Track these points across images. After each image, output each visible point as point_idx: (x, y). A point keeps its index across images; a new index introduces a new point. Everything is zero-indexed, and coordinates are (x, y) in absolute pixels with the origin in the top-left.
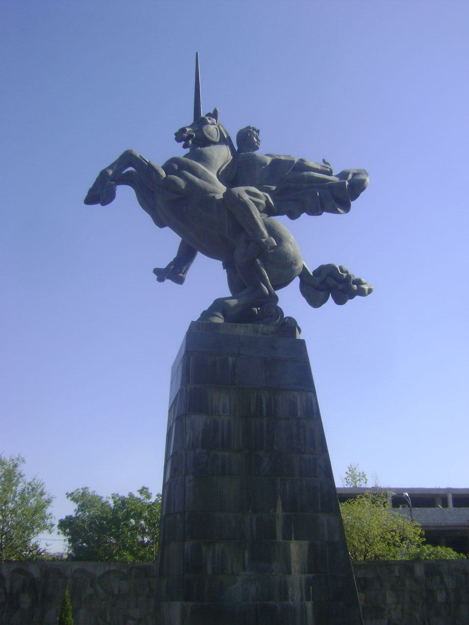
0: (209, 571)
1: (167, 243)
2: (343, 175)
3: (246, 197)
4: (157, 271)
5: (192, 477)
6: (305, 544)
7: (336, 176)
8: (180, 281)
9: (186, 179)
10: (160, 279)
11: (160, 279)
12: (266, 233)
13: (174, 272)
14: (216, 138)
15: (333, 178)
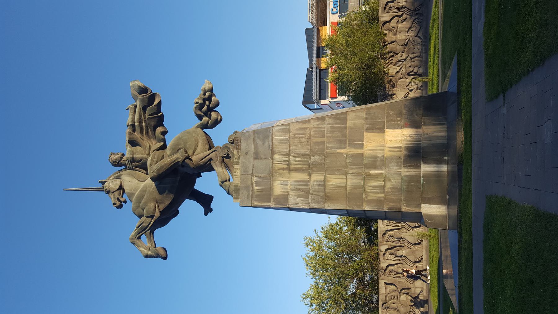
0: (383, 195)
1: (189, 207)
2: (135, 99)
3: (155, 167)
4: (206, 214)
5: (326, 205)
6: (367, 135)
7: (136, 101)
8: (210, 198)
9: (146, 204)
10: (211, 210)
11: (211, 210)
12: (176, 156)
13: (206, 201)
14: (118, 182)
15: (138, 104)
